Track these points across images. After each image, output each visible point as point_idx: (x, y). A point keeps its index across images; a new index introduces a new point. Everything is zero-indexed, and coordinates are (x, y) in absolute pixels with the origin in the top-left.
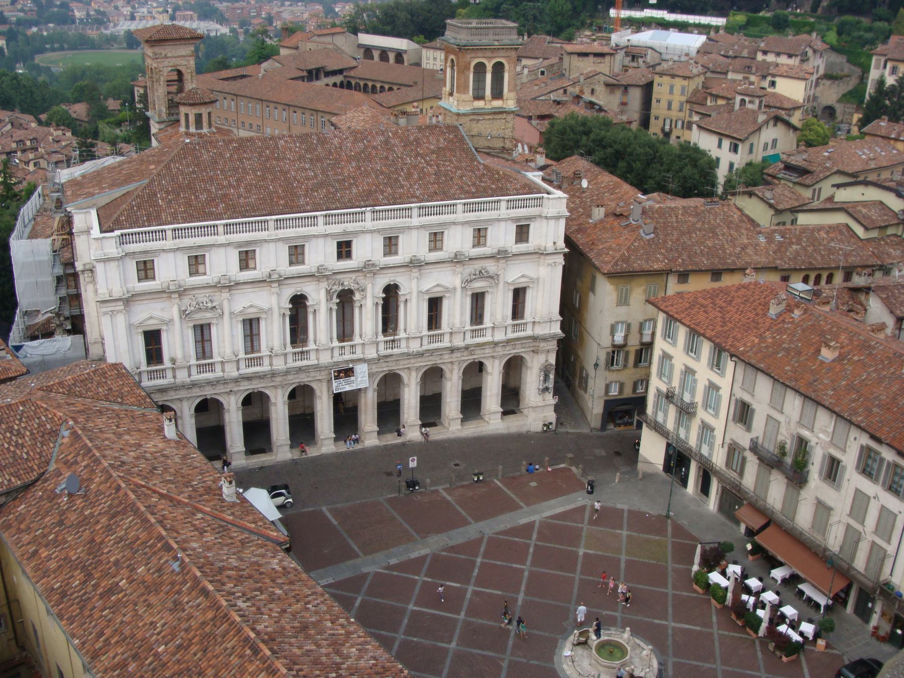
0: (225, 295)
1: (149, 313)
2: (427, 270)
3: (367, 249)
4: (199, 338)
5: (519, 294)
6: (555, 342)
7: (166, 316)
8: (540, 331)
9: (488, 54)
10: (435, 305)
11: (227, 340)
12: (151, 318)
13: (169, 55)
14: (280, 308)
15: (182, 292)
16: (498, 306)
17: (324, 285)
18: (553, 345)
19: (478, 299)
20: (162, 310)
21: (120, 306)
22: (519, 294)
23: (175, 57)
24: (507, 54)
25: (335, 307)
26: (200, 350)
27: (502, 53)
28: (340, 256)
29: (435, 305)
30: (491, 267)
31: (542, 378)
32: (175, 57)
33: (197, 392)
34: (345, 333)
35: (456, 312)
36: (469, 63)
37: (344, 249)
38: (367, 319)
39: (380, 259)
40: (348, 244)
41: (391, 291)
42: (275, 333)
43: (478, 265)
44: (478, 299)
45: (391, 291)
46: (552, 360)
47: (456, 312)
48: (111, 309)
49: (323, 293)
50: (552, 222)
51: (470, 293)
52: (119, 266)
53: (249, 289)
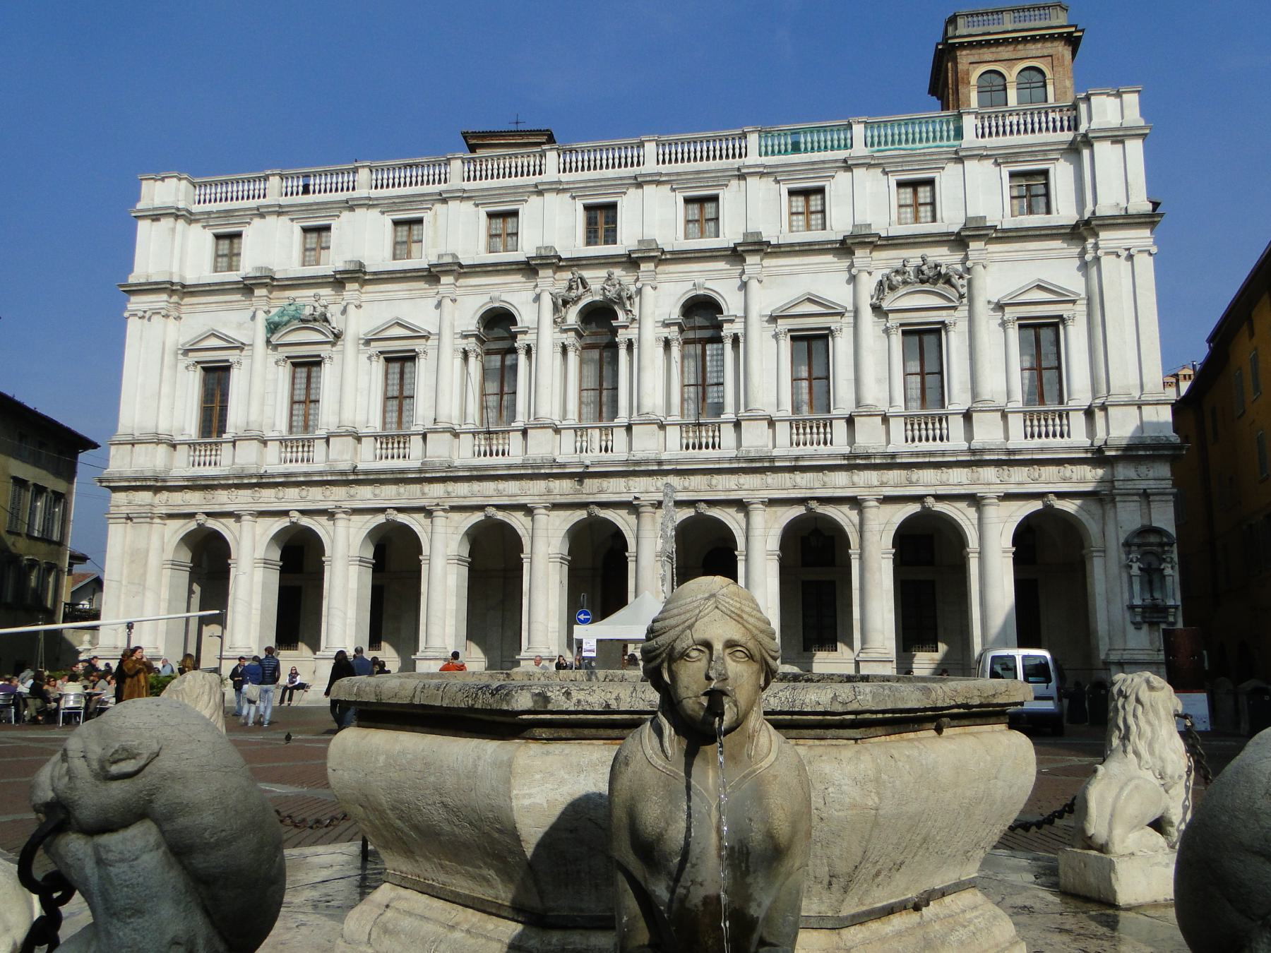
3: (651, 216)
4: (301, 395)
5: (1042, 335)
6: (1164, 470)
10: (811, 345)
17: (552, 283)
18: (1159, 475)
19: (924, 340)
22: (1042, 335)
26: (298, 421)
28: (591, 238)
29: (811, 345)
30: (944, 257)
31: (1135, 570)
37: (601, 218)
38: (653, 376)
40: (610, 209)
41: (702, 313)
42: (448, 386)
43: (913, 256)
44: (924, 340)
45: (702, 313)
46: (1164, 517)
49: (547, 301)
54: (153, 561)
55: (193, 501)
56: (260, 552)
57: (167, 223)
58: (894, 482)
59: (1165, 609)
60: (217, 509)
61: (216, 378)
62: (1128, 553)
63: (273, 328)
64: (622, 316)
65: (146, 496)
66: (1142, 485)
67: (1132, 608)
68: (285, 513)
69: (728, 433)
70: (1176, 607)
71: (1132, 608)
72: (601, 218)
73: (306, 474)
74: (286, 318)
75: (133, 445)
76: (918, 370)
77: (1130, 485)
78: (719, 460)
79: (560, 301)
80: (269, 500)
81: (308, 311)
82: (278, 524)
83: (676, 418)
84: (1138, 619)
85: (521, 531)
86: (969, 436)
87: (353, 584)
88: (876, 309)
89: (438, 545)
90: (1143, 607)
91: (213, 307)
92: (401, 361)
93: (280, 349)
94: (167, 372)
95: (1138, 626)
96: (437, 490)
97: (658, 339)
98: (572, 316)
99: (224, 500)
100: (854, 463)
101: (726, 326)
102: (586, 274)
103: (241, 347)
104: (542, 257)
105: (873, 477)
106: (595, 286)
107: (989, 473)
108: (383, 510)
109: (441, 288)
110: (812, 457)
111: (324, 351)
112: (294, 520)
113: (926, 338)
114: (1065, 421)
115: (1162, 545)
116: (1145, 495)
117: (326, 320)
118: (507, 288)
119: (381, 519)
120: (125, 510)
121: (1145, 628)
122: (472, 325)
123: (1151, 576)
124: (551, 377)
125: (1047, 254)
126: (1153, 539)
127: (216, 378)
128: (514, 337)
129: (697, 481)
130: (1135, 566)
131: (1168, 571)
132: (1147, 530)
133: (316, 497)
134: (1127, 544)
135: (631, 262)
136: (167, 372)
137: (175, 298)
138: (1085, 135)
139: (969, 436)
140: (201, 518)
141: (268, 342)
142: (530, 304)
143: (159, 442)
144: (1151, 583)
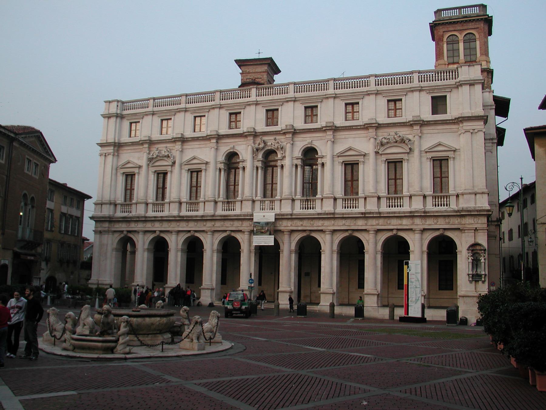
0: (178, 146)
2: (341, 135)
7: (139, 163)
8: (466, 203)
9: (458, 27)
10: (351, 168)
12: (129, 162)
13: (251, 71)
14: (216, 162)
16: (417, 176)
19: (394, 166)
20: (139, 159)
22: (440, 164)
23: (254, 73)
24: (476, 26)
25: (260, 164)
27: (471, 25)
29: (351, 168)
31: (470, 260)
32: (254, 73)
34: (269, 190)
35: (372, 178)
36: (443, 36)
39: (300, 124)
43: (392, 131)
44: (394, 166)
47: (372, 178)
48: (105, 152)
49: (250, 149)
50: (466, 88)
51: (384, 158)
52: (116, 121)
53: (196, 144)
54: (109, 249)
55: (123, 227)
56: (146, 246)
57: (113, 120)
58: (381, 224)
59: (480, 276)
60: (131, 229)
62: (468, 253)
63: (150, 160)
64: (279, 156)
65: (106, 225)
66: (476, 226)
67: (469, 275)
68: (155, 232)
69: (318, 203)
70: (485, 275)
71: (469, 275)
72: (272, 115)
73: (162, 217)
74: (155, 156)
75: (102, 205)
76: (394, 177)
77: (471, 226)
78: (314, 215)
79: (255, 150)
80: (149, 226)
81: (163, 153)
82: (152, 236)
83: (299, 196)
84: (471, 279)
85: (240, 240)
86: (410, 206)
87: (179, 259)
88: (377, 153)
90: (473, 275)
91: (129, 151)
92: (195, 173)
94: (113, 176)
95: (471, 282)
96: (209, 224)
97: (292, 165)
98: (260, 156)
99: (133, 226)
100: (365, 216)
101: (319, 159)
102: (265, 138)
103: (140, 167)
104: (248, 132)
105: (374, 222)
106: (269, 144)
107: (418, 221)
108: (189, 231)
110: (349, 214)
111: (169, 169)
113: (397, 164)
114: (448, 200)
115: (481, 250)
116: (476, 230)
117: (169, 157)
119: (189, 235)
121: (474, 282)
122: (221, 158)
123: (476, 263)
124: (249, 181)
125: (445, 131)
126: (478, 248)
128: (238, 163)
129: (305, 223)
130: (470, 258)
131: (483, 260)
132: (476, 245)
133: (166, 226)
134: (468, 250)
135: (284, 133)
136: (113, 176)
137: (116, 149)
138: (459, 82)
139: (410, 206)
142: (245, 150)
143: (111, 204)
144: (477, 265)
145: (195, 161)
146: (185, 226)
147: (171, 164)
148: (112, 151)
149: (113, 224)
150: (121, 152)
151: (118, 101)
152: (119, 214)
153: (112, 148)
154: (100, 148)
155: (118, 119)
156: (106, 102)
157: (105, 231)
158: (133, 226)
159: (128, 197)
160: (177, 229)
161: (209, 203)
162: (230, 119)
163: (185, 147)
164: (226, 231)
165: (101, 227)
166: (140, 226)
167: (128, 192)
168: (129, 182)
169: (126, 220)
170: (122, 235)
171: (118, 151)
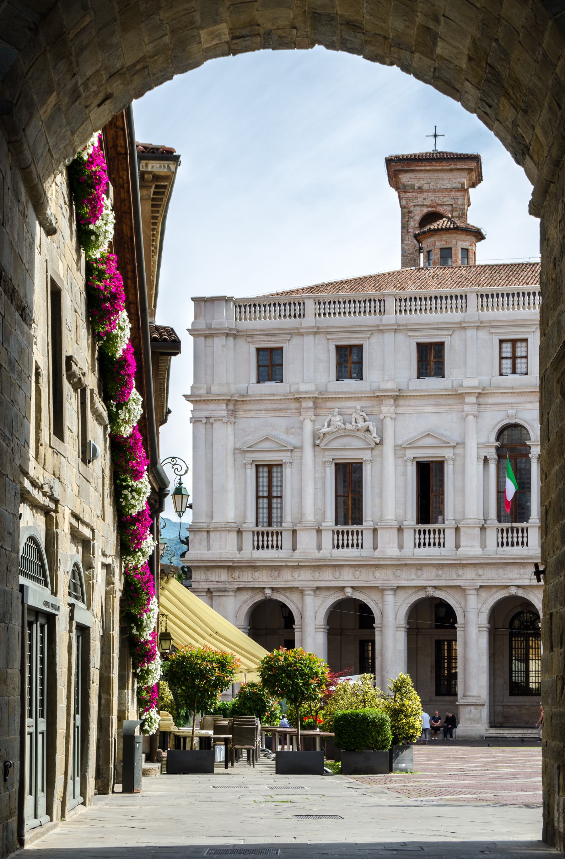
1: (265, 427)
11: (390, 494)
15: (319, 401)
20: (287, 432)
21: (221, 411)
33: (327, 578)
48: (207, 414)
57: (218, 342)
61: (268, 474)
68: (343, 588)
89: (472, 616)
91: (263, 414)
93: (327, 453)
96: (470, 573)
109: (466, 408)
111: (366, 456)
112: (349, 594)
117: (368, 430)
118: (520, 407)
120: (205, 585)
127: (268, 474)
137: (231, 407)
140: (268, 592)
141: (315, 446)
145: (428, 441)
146: (413, 577)
147: (373, 445)
148: (224, 413)
149: (236, 574)
150: (240, 414)
151: (226, 300)
152: (249, 553)
153: (224, 407)
154: (190, 406)
155: (231, 339)
156: (196, 300)
157: (220, 590)
158: (286, 578)
159: (264, 513)
160: (396, 583)
161: (469, 531)
162: (500, 352)
163: (400, 410)
164: (507, 587)
165: (207, 581)
166: (304, 578)
167: (264, 503)
168: (264, 481)
169: (275, 568)
170: (259, 597)
171: (234, 411)
